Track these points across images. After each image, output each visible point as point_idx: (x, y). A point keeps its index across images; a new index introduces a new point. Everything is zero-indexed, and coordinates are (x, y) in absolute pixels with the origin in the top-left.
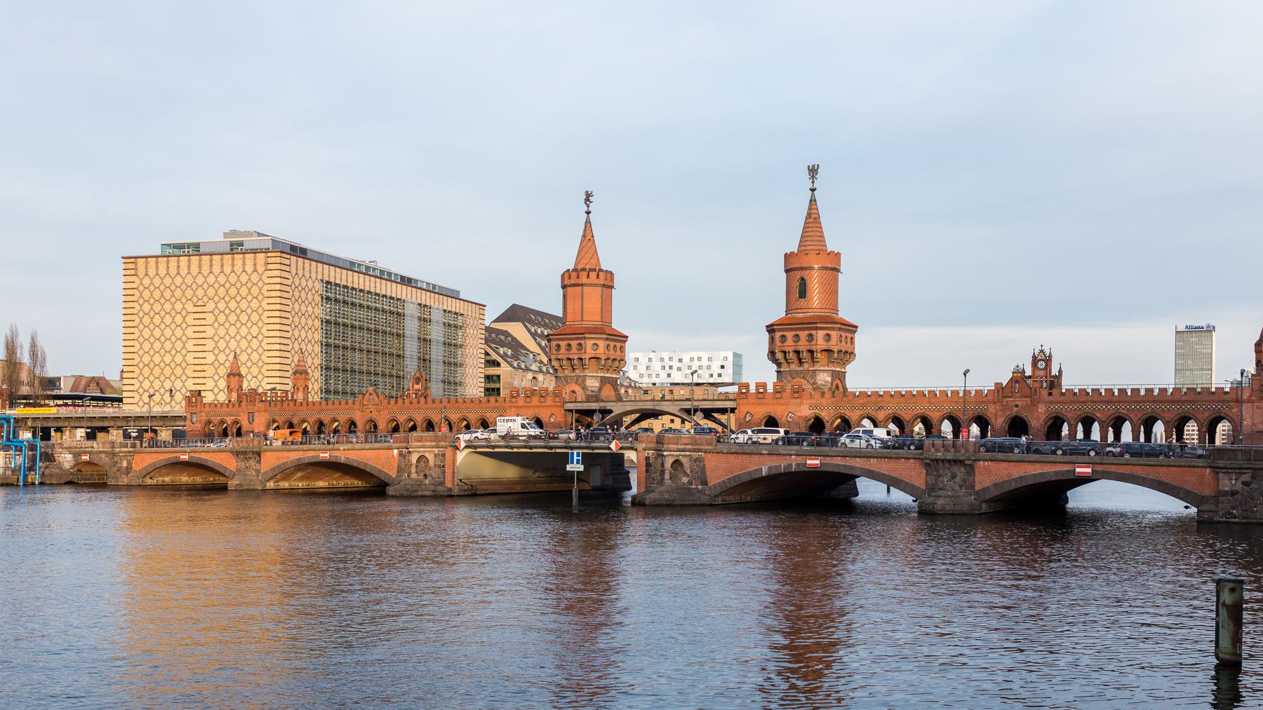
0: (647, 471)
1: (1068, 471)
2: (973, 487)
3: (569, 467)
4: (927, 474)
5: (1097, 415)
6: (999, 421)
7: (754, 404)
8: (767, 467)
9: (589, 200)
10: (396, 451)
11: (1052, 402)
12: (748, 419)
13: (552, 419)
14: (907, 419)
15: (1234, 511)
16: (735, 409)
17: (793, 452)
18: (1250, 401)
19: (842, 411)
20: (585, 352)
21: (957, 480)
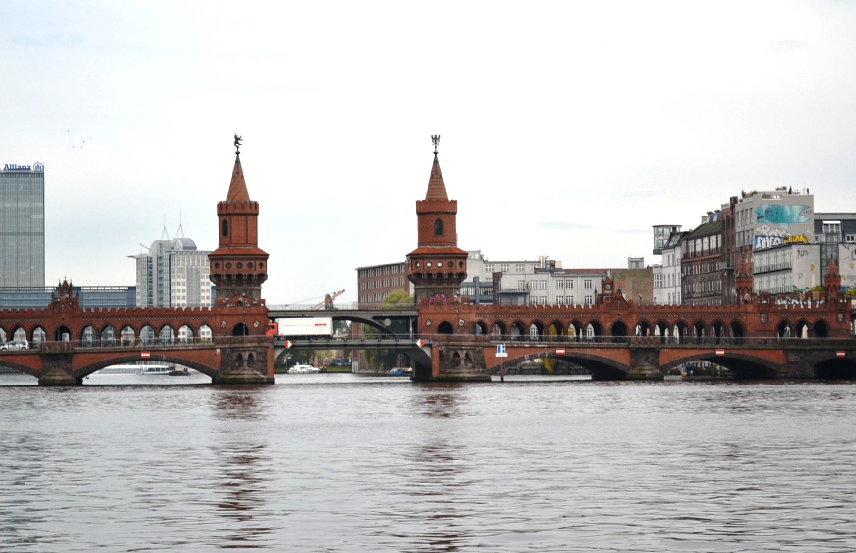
0: (441, 360)
1: (711, 354)
2: (659, 364)
3: (497, 355)
4: (631, 357)
5: (668, 320)
6: (608, 325)
7: (432, 314)
8: (528, 355)
9: (238, 143)
10: (218, 351)
11: (640, 313)
12: (428, 324)
13: (255, 324)
14: (547, 324)
15: (797, 372)
16: (418, 316)
17: (546, 346)
18: (753, 313)
19: (500, 319)
20: (256, 270)
21: (649, 360)
